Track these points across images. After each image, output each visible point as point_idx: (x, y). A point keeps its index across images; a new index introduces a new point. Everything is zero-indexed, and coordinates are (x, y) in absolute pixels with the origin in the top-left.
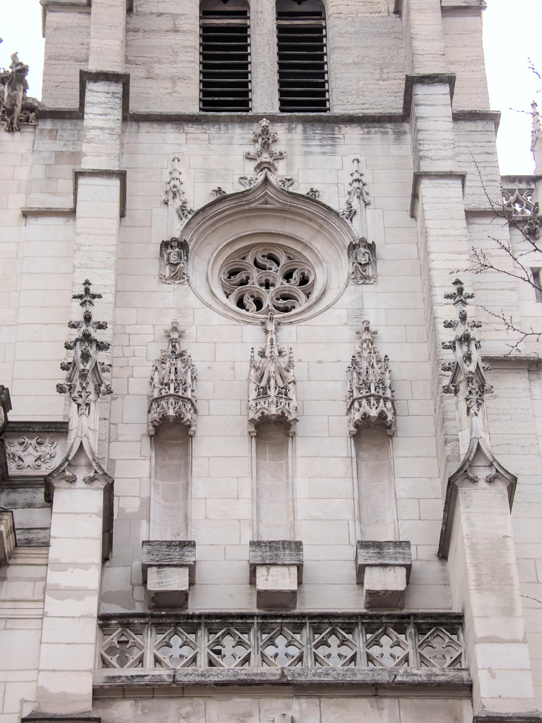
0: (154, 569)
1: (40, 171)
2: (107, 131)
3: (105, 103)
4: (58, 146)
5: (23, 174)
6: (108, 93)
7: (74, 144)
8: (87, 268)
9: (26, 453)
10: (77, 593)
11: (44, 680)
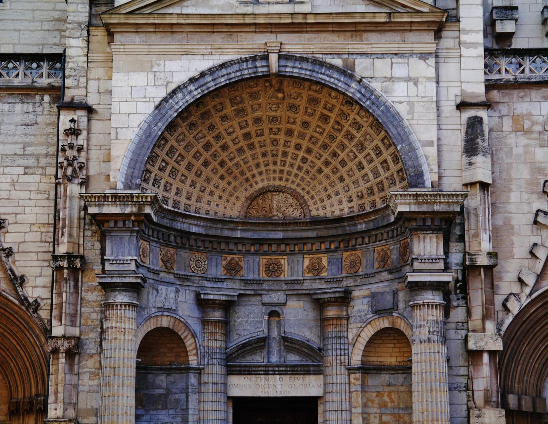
0: (499, 21)
10: (473, 45)
11: (464, 86)
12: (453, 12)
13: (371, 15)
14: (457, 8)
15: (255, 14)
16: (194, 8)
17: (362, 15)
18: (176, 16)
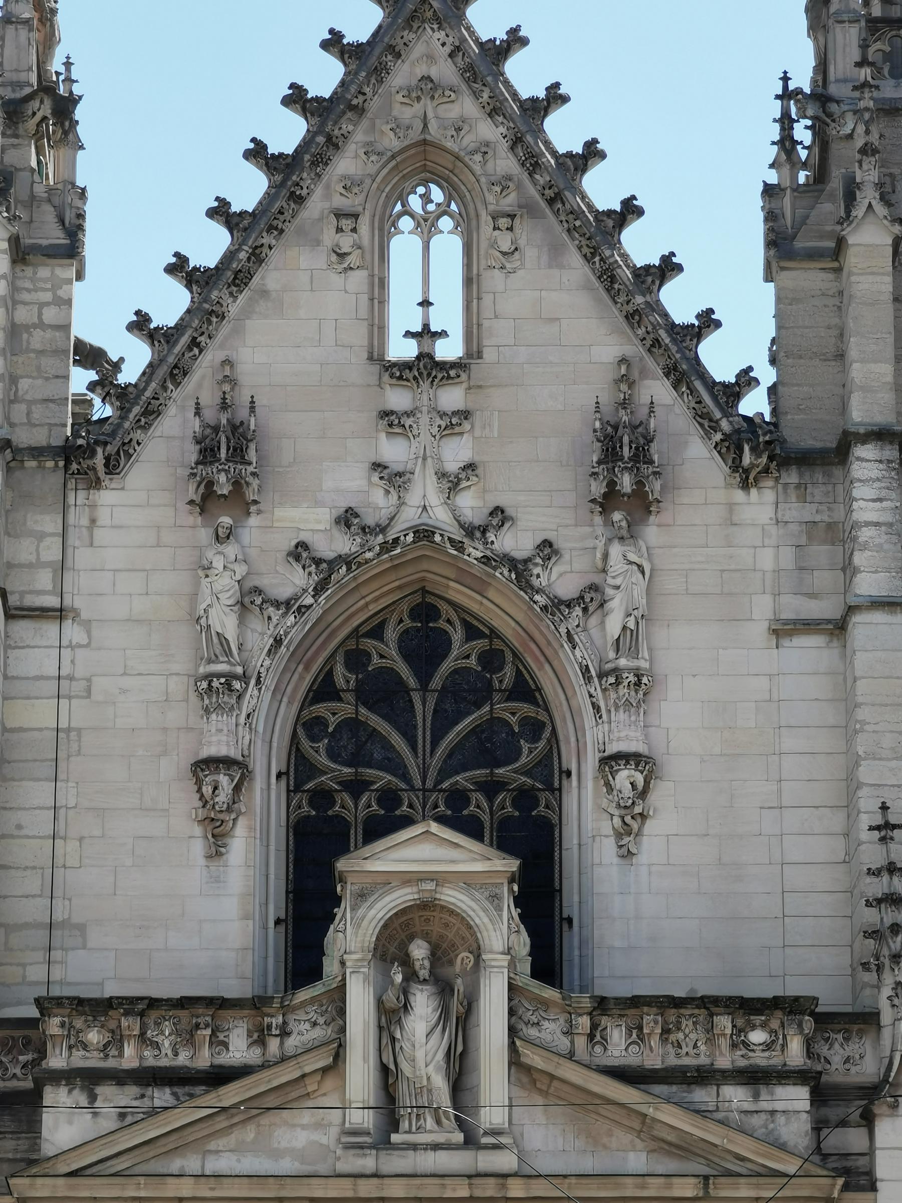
1: (788, 557)
2: (883, 528)
3: (878, 479)
4: (808, 512)
5: (766, 560)
6: (881, 462)
7: (829, 509)
8: (875, 759)
9: (832, 1052)
12: (862, 1162)
13: (662, 1180)
14: (870, 1153)
15: (383, 1176)
16: (234, 1157)
17: (639, 1180)
18: (191, 1180)
